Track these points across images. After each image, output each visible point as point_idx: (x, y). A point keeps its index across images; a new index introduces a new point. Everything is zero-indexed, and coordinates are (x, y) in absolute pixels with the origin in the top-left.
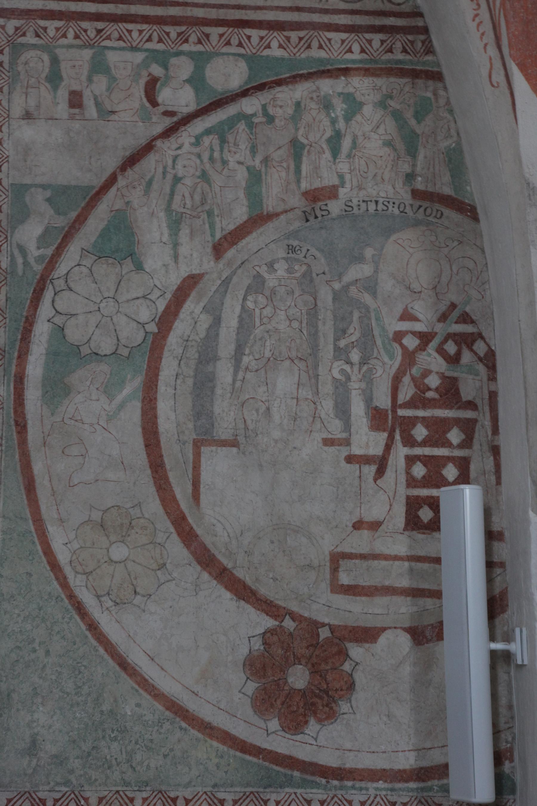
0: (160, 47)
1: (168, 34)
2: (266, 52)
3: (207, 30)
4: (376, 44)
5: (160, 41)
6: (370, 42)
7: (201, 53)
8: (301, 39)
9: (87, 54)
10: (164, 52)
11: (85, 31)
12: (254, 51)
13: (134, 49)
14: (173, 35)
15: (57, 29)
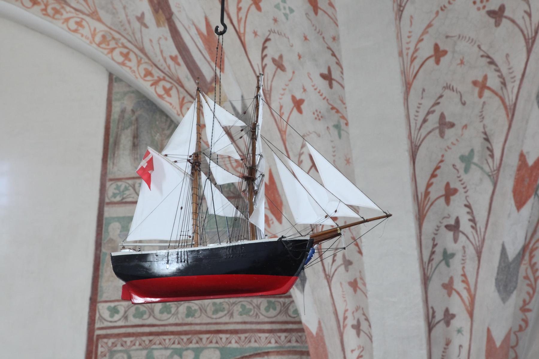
0: (179, 346)
1: (182, 340)
2: (229, 346)
3: (201, 336)
4: (283, 338)
5: (179, 343)
6: (280, 337)
7: (198, 348)
8: (246, 338)
9: (144, 353)
10: (180, 349)
11: (144, 341)
12: (223, 345)
13: (166, 348)
14: (185, 340)
15: (131, 342)
